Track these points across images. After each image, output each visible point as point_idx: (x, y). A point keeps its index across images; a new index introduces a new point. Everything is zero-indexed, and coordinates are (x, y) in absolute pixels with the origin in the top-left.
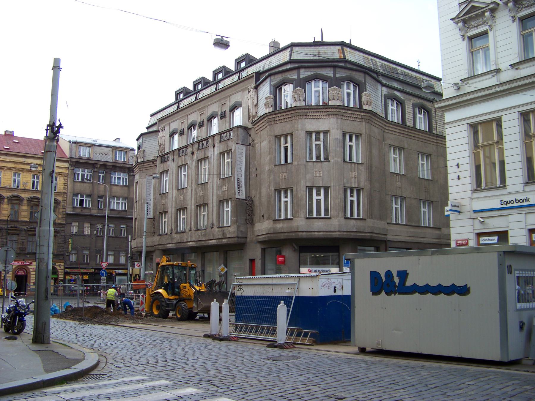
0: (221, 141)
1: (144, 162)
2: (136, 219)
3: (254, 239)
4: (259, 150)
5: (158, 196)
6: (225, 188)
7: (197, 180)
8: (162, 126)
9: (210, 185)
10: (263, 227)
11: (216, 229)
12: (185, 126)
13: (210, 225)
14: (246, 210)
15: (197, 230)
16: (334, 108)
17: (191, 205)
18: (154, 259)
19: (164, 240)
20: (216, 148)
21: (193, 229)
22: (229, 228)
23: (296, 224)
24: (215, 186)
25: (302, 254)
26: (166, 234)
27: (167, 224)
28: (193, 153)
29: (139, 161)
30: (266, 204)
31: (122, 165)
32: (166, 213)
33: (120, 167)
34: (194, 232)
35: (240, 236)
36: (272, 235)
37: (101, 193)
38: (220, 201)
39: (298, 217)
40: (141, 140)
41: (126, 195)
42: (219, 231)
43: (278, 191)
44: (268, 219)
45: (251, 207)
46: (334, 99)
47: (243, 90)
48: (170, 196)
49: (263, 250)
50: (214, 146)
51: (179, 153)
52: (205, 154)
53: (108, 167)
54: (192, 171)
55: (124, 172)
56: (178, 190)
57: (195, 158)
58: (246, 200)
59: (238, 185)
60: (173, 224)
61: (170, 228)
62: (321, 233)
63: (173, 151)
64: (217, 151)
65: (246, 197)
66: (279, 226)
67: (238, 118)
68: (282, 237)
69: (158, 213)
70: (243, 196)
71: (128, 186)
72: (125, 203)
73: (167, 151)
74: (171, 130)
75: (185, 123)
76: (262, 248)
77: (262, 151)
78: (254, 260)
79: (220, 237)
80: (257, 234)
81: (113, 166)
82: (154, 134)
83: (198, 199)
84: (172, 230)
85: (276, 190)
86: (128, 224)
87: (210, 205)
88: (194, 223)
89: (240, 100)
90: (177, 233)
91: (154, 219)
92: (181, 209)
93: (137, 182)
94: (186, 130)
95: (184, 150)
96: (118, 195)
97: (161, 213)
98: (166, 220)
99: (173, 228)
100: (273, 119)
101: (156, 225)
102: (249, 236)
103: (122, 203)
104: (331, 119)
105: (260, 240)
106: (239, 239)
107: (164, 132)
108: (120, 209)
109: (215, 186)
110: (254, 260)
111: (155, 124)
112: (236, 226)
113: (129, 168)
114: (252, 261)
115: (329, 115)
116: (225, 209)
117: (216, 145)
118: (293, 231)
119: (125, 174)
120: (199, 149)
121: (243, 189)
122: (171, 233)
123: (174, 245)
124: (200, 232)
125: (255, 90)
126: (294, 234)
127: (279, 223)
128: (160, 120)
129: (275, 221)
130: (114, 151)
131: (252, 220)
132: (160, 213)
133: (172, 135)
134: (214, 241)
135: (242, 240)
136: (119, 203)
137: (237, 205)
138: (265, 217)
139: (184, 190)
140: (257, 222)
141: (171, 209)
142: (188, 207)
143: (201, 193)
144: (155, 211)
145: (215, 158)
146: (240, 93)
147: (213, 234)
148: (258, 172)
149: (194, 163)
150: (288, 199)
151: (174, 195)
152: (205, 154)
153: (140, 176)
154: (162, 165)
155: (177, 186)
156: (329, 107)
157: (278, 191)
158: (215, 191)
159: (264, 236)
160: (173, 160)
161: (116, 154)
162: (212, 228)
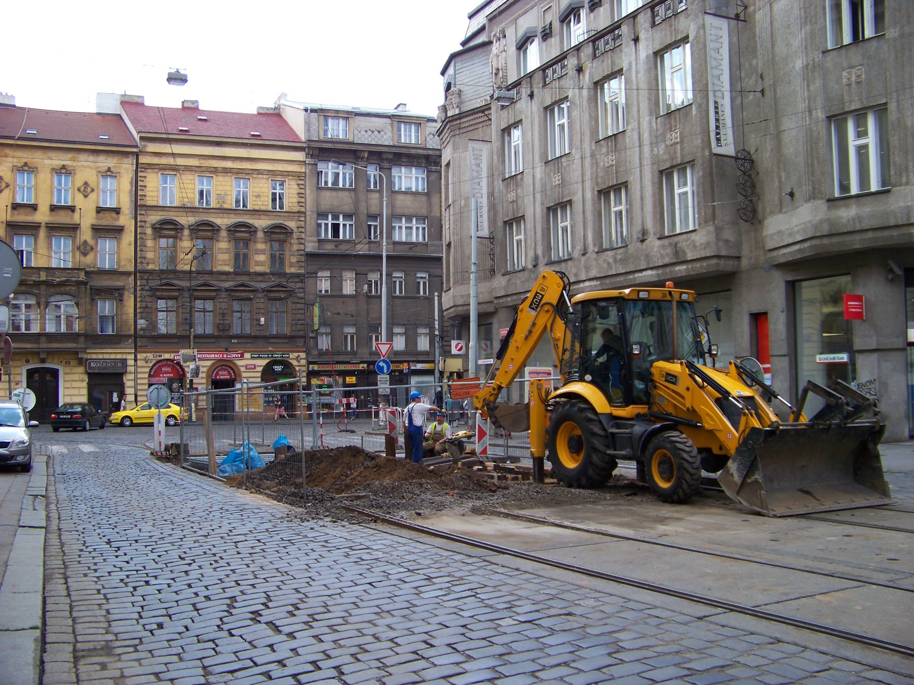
0: (653, 25)
1: (461, 116)
2: (449, 245)
3: (762, 258)
4: (767, 25)
5: (499, 185)
6: (675, 136)
7: (594, 131)
8: (497, 30)
9: (631, 138)
10: (791, 225)
11: (653, 243)
12: (553, 17)
13: (636, 234)
14: (739, 185)
15: (601, 251)
17: (584, 195)
18: (494, 331)
19: (518, 283)
20: (642, 45)
21: (591, 248)
23: (902, 204)
24: (646, 135)
25: (908, 289)
26: (523, 270)
27: (523, 246)
28: (580, 70)
29: (450, 114)
30: (801, 160)
31: (413, 151)
32: (519, 219)
33: (409, 156)
34: (594, 256)
35: (724, 253)
36: (826, 241)
37: (374, 210)
38: (661, 172)
39: (907, 183)
40: (451, 71)
41: (424, 212)
42: (663, 247)
43: (837, 119)
44: (812, 197)
45: (750, 176)
48: (528, 179)
49: (792, 287)
50: (636, 40)
51: (545, 77)
52: (613, 63)
53: (385, 156)
54: (582, 116)
55: (418, 166)
56: (547, 163)
57: (586, 79)
58: (736, 158)
59: (717, 120)
60: (539, 243)
61: (531, 254)
63: (530, 76)
64: (645, 50)
65: (737, 153)
66: (847, 214)
68: (857, 243)
69: (500, 224)
70: (728, 148)
71: (427, 194)
72: (424, 229)
73: (512, 78)
74: (520, 33)
75: (554, 8)
76: (787, 282)
77: (776, 25)
78: (765, 314)
79: (667, 260)
80: (770, 245)
81: (395, 154)
82: (480, 50)
83: (601, 174)
84: (536, 258)
85: (829, 118)
86: (432, 271)
87: (635, 187)
88: (594, 235)
90: (550, 263)
91: (491, 239)
92: (558, 207)
93: (448, 165)
94: (556, 25)
95: (558, 67)
96: (407, 211)
97: (508, 223)
98: (522, 237)
99: (540, 252)
101: (497, 250)
102: (745, 252)
103: (418, 228)
105: (782, 260)
106: (722, 262)
107: (503, 41)
108: (414, 240)
109: (646, 135)
110: (765, 314)
111: (482, 30)
112: (711, 228)
113: (427, 157)
114: (759, 319)
116: (677, 191)
117: (642, 36)
118: (892, 222)
119: (421, 171)
120: (595, 57)
121: (728, 133)
122: (534, 266)
124: (610, 253)
126: (895, 233)
127: (847, 206)
128: (492, 18)
129: (831, 200)
130: (395, 124)
131: (754, 211)
132: (505, 222)
133: (522, 45)
134: (649, 272)
135: (729, 266)
136: (411, 228)
137: (711, 174)
138: (797, 195)
139: (564, 160)
140: (772, 213)
141: (533, 209)
142: (574, 199)
143: (610, 160)
144: (492, 221)
145: (642, 68)
147: (647, 256)
148: (768, 81)
149: (585, 92)
150: (871, 140)
151: (538, 176)
152: (613, 63)
153: (455, 149)
154: (504, 113)
155: (544, 154)
157: (837, 119)
158: (646, 150)
159: (797, 247)
160: (531, 96)
161: (399, 130)
162: (643, 241)
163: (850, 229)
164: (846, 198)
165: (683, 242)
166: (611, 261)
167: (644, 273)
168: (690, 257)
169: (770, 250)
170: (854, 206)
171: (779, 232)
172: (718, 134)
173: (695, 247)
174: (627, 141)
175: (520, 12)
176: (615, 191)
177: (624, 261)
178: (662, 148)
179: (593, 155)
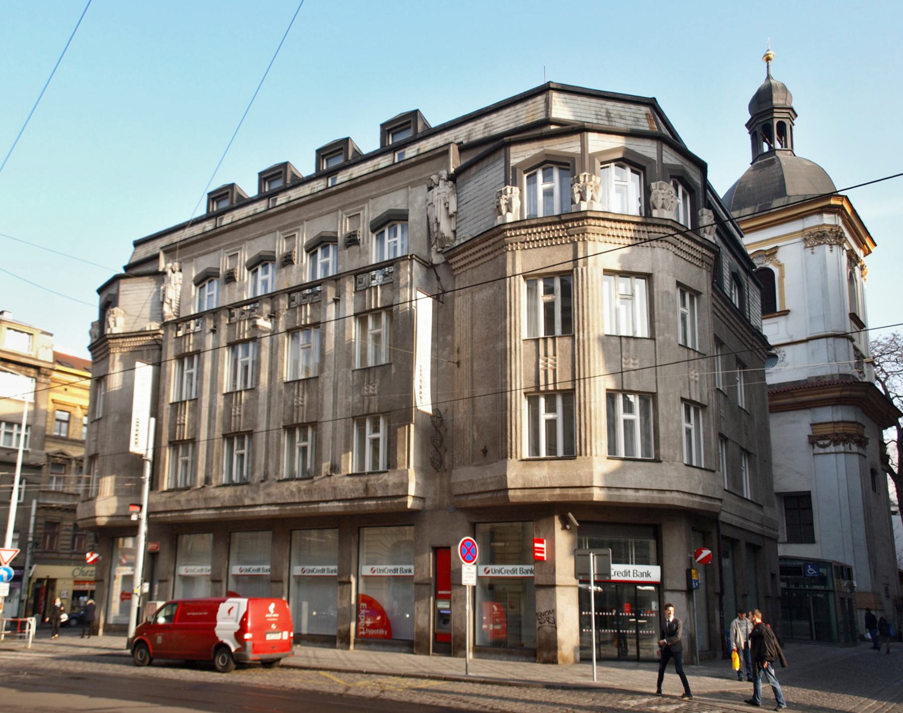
16: (663, 226)
46: (663, 207)
62: (641, 493)
79: (356, 495)
89: (403, 207)
104: (657, 249)
105: (470, 505)
115: (650, 240)
118: (578, 484)
126: (579, 492)
134: (336, 504)
138: (491, 452)
140: (462, 464)
146: (402, 192)
156: (656, 221)
159: (489, 495)
167: (329, 504)
169: (456, 496)
170: (546, 468)
171: (469, 481)
172: (421, 393)
175: (201, 252)
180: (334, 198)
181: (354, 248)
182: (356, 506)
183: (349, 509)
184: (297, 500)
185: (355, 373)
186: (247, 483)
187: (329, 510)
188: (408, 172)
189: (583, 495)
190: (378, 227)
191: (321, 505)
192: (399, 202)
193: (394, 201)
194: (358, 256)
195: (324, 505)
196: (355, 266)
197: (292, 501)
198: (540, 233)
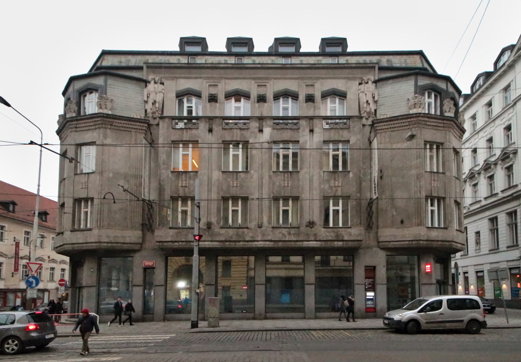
22: (349, 230)
47: (349, 79)
50: (312, 131)
67: (332, 108)
79: (330, 238)
100: (424, 123)
118: (448, 239)
123: (216, 243)
125: (374, 84)
126: (448, 244)
134: (315, 242)
138: (406, 221)
163: (434, 239)
164: (433, 228)
165: (343, 232)
166: (286, 233)
167: (310, 242)
168: (346, 238)
173: (351, 235)
174: (301, 177)
176: (284, 199)
177: (298, 234)
178: (327, 186)
179: (270, 177)
180: (296, 71)
181: (310, 104)
182: (329, 244)
183: (323, 246)
184: (287, 239)
185: (325, 173)
186: (247, 228)
187: (311, 246)
188: (347, 71)
189: (450, 245)
190: (325, 95)
191: (304, 243)
192: (340, 85)
193: (339, 85)
194: (313, 109)
195: (307, 243)
196: (310, 113)
197: (284, 239)
198: (433, 122)
